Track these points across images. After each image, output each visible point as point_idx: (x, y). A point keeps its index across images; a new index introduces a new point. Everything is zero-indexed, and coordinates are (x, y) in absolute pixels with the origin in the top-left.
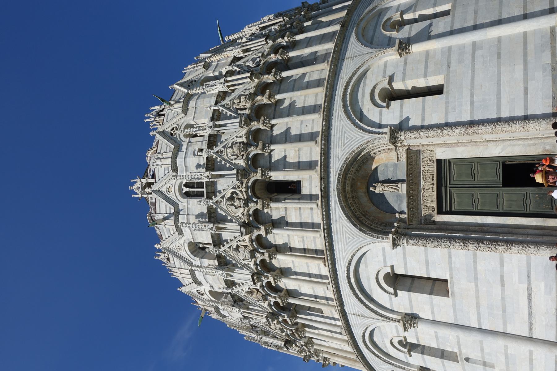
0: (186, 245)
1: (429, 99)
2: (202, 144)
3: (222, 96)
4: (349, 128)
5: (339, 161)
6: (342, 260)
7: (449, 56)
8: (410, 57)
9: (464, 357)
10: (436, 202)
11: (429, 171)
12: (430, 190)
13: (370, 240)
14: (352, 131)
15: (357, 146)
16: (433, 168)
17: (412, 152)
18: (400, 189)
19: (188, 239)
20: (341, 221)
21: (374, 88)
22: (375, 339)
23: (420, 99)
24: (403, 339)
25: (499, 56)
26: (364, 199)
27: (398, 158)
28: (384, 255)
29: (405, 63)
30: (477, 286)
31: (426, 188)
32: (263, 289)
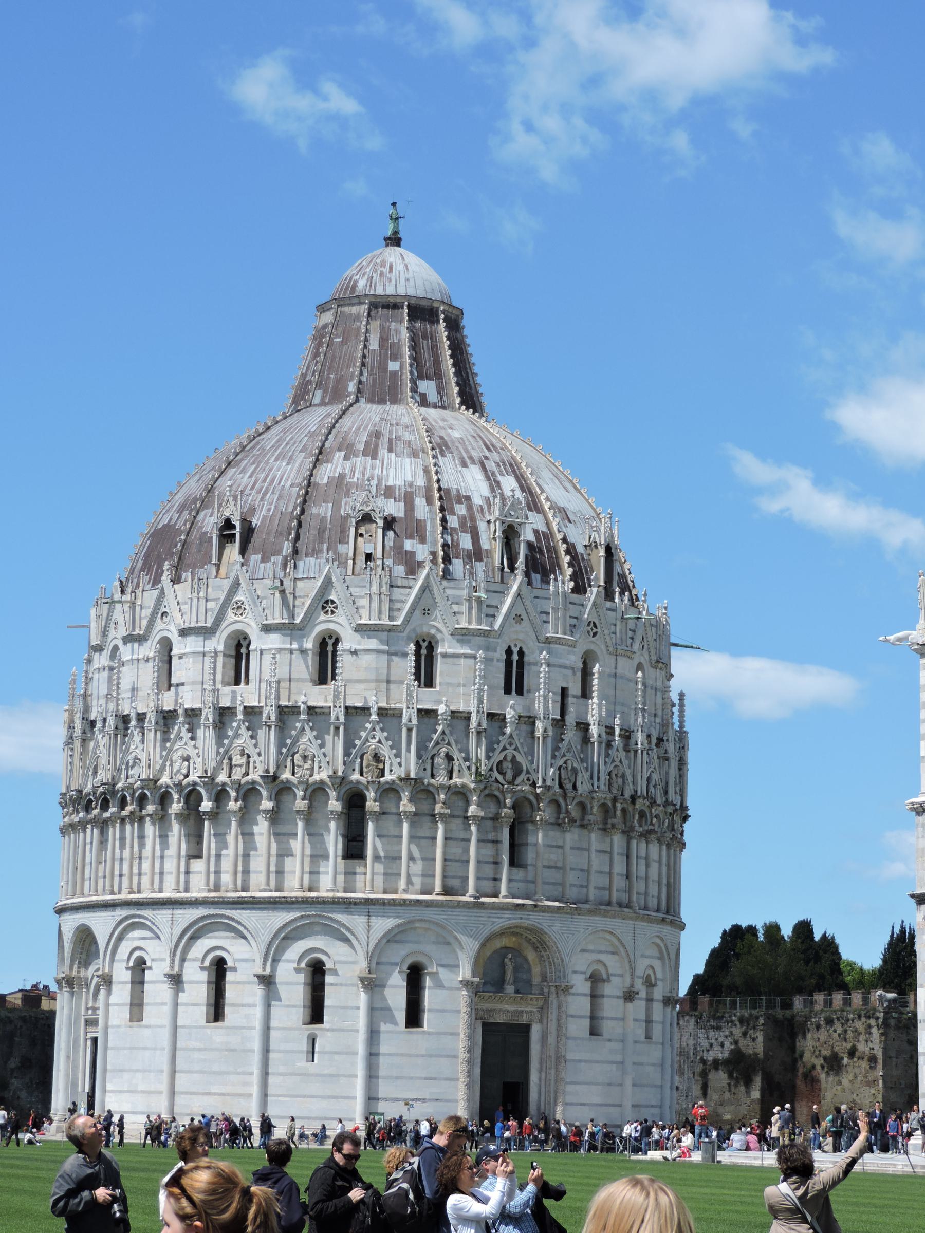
0: (433, 631)
1: (587, 1022)
2: (575, 696)
3: (627, 735)
7: (616, 1041)
8: (621, 1001)
9: (317, 1032)
16: (524, 1020)
19: (443, 640)
21: (604, 965)
22: (317, 928)
23: (589, 1014)
24: (329, 965)
25: (610, 1084)
26: (499, 944)
29: (618, 997)
30: (423, 1056)
32: (387, 783)
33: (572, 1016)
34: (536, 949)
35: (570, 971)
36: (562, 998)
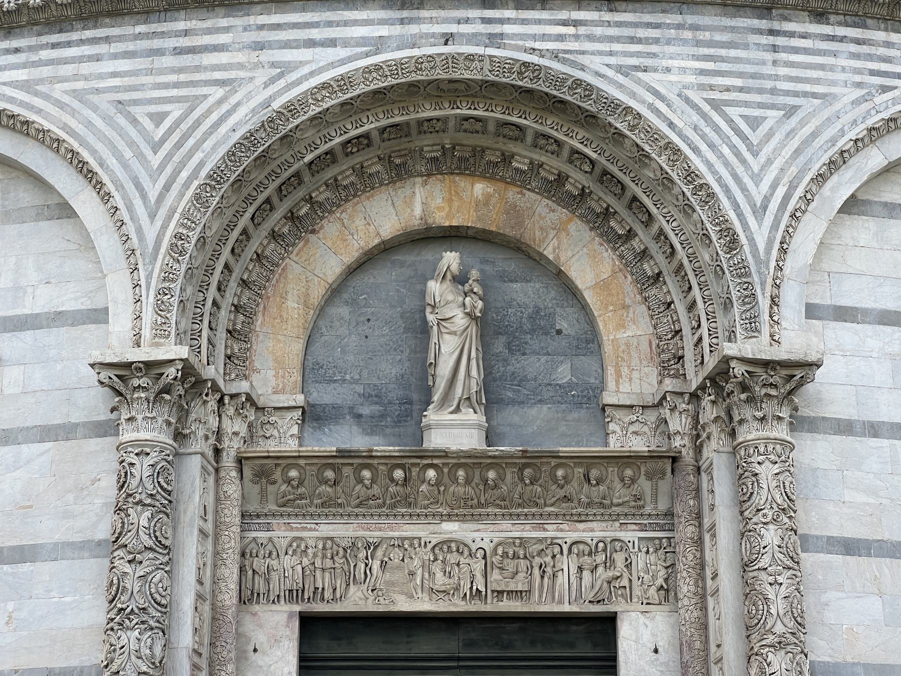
4: (814, 135)
5: (619, 69)
6: (21, 75)
10: (371, 607)
11: (548, 573)
12: (440, 580)
13: (151, 235)
14: (797, 152)
15: (710, 179)
16: (565, 593)
17: (664, 486)
18: (445, 416)
20: (261, 76)
27: (631, 407)
28: (57, 319)
31: (453, 558)
33: (849, 547)
34: (600, 221)
35: (792, 299)
36: (749, 433)
